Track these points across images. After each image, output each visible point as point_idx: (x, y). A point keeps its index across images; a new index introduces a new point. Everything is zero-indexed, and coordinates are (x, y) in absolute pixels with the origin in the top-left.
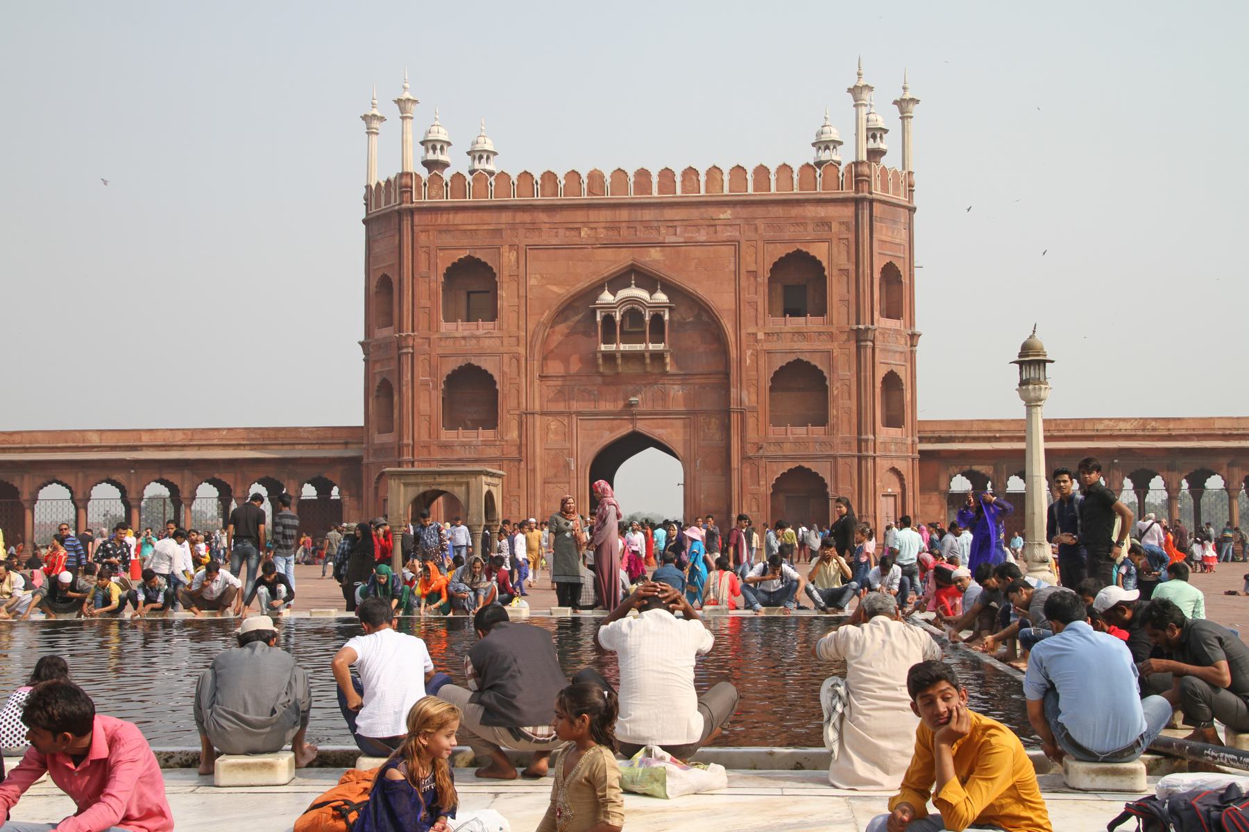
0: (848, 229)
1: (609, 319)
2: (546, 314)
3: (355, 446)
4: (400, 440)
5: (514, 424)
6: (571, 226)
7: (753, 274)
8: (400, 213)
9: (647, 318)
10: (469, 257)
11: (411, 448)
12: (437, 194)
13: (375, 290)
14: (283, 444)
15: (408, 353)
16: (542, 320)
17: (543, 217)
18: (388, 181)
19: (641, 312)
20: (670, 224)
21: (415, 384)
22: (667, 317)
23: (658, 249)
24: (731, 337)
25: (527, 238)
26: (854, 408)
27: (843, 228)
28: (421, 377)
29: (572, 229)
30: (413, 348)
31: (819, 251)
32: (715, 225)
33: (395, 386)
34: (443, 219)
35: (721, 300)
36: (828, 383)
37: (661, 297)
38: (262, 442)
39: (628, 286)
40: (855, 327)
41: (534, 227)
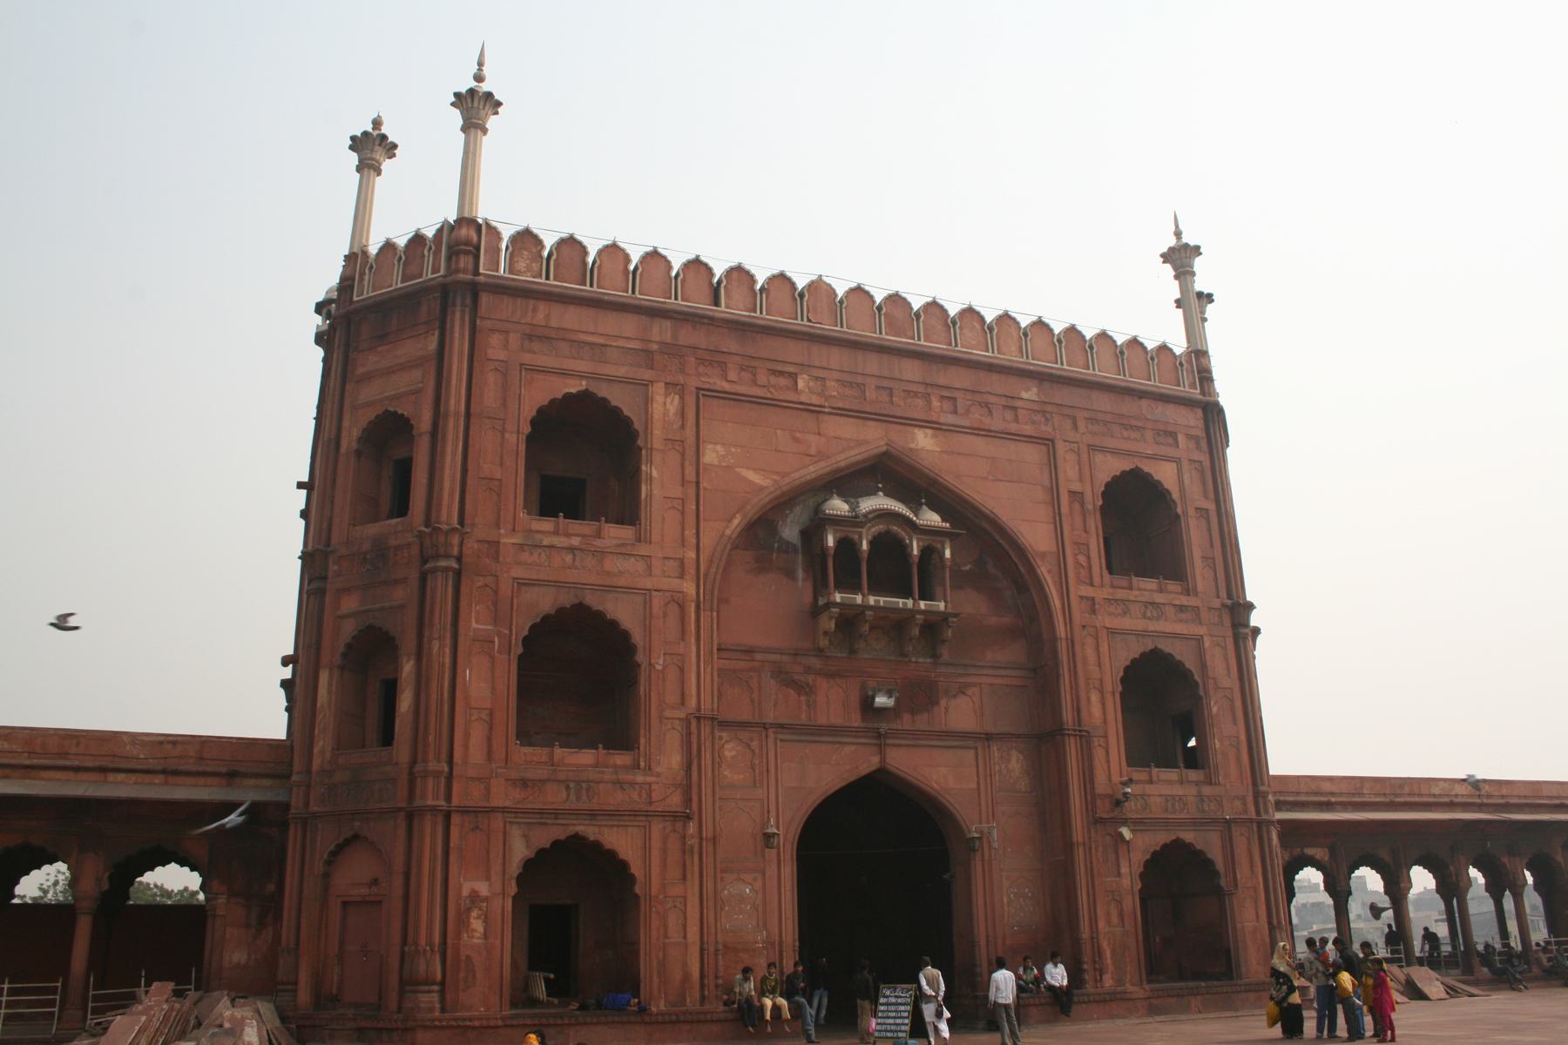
0: (1199, 448)
1: (847, 547)
2: (736, 522)
3: (251, 782)
4: (414, 762)
5: (673, 739)
6: (779, 368)
7: (1076, 496)
8: (445, 292)
9: (915, 552)
10: (585, 396)
11: (443, 780)
12: (529, 268)
13: (355, 445)
14: (77, 769)
15: (446, 569)
16: (728, 532)
17: (730, 344)
18: (418, 239)
19: (904, 540)
20: (946, 394)
21: (461, 639)
22: (948, 554)
23: (929, 432)
24: (1056, 602)
25: (699, 375)
26: (1243, 737)
27: (1192, 445)
28: (476, 623)
29: (782, 373)
30: (459, 559)
31: (1165, 474)
32: (1015, 409)
33: (408, 642)
34: (542, 314)
35: (1035, 535)
36: (1201, 692)
37: (931, 518)
38: (27, 762)
39: (872, 492)
40: (1229, 602)
41: (714, 359)
